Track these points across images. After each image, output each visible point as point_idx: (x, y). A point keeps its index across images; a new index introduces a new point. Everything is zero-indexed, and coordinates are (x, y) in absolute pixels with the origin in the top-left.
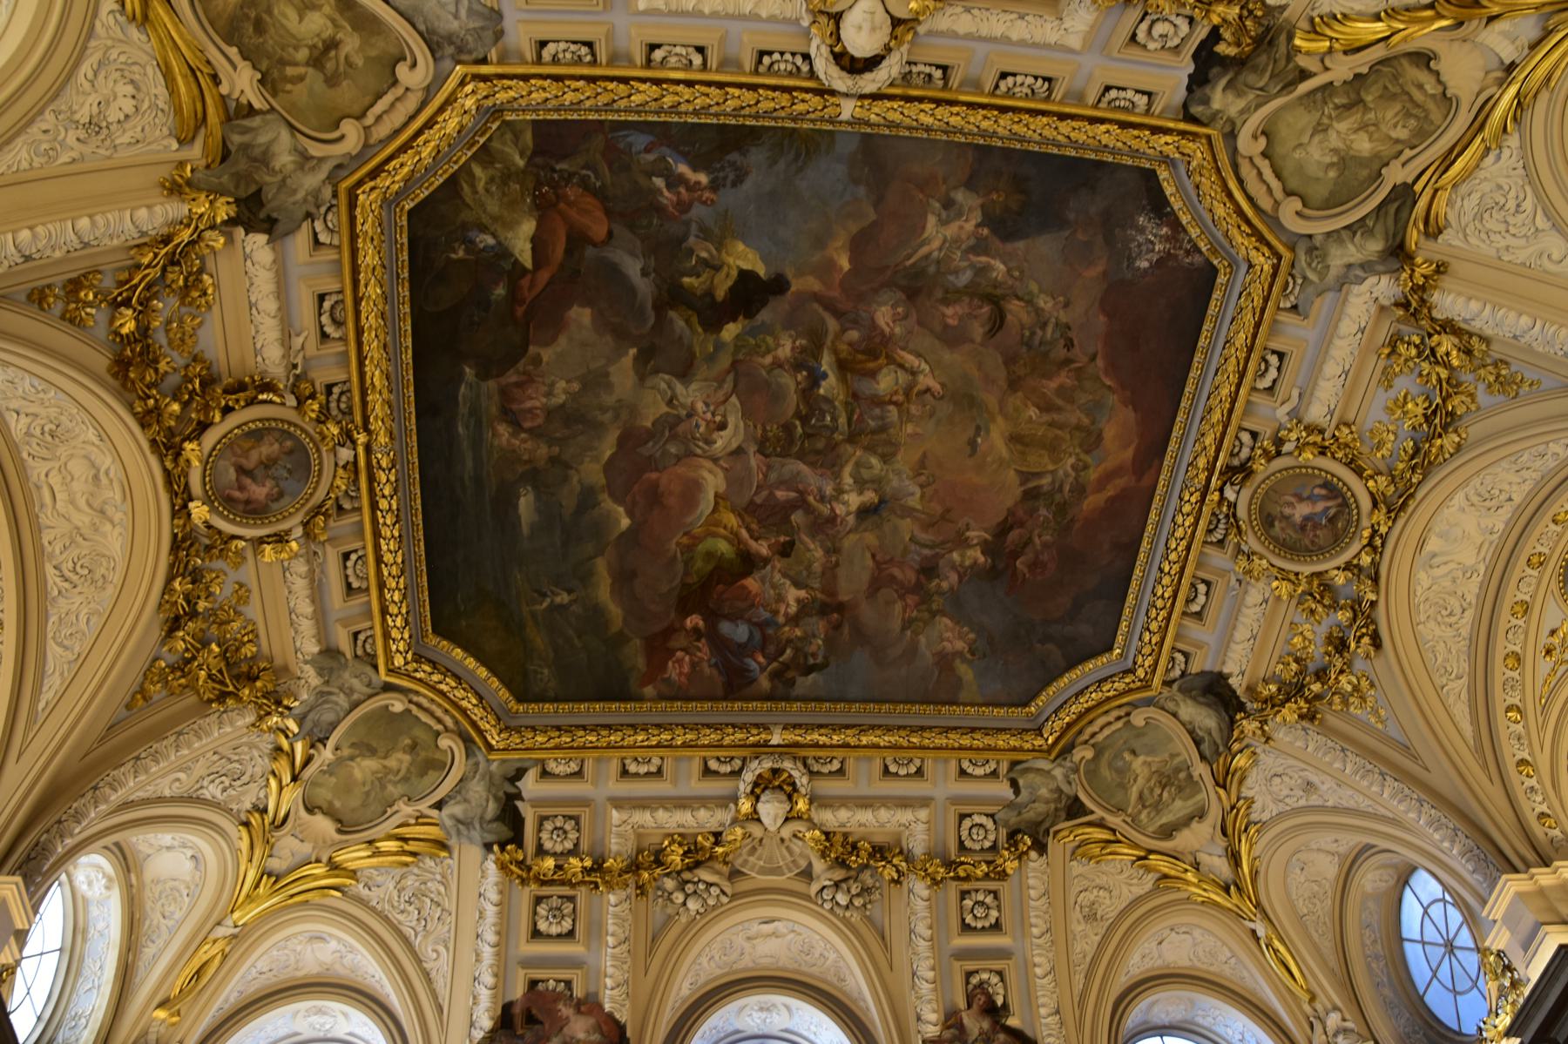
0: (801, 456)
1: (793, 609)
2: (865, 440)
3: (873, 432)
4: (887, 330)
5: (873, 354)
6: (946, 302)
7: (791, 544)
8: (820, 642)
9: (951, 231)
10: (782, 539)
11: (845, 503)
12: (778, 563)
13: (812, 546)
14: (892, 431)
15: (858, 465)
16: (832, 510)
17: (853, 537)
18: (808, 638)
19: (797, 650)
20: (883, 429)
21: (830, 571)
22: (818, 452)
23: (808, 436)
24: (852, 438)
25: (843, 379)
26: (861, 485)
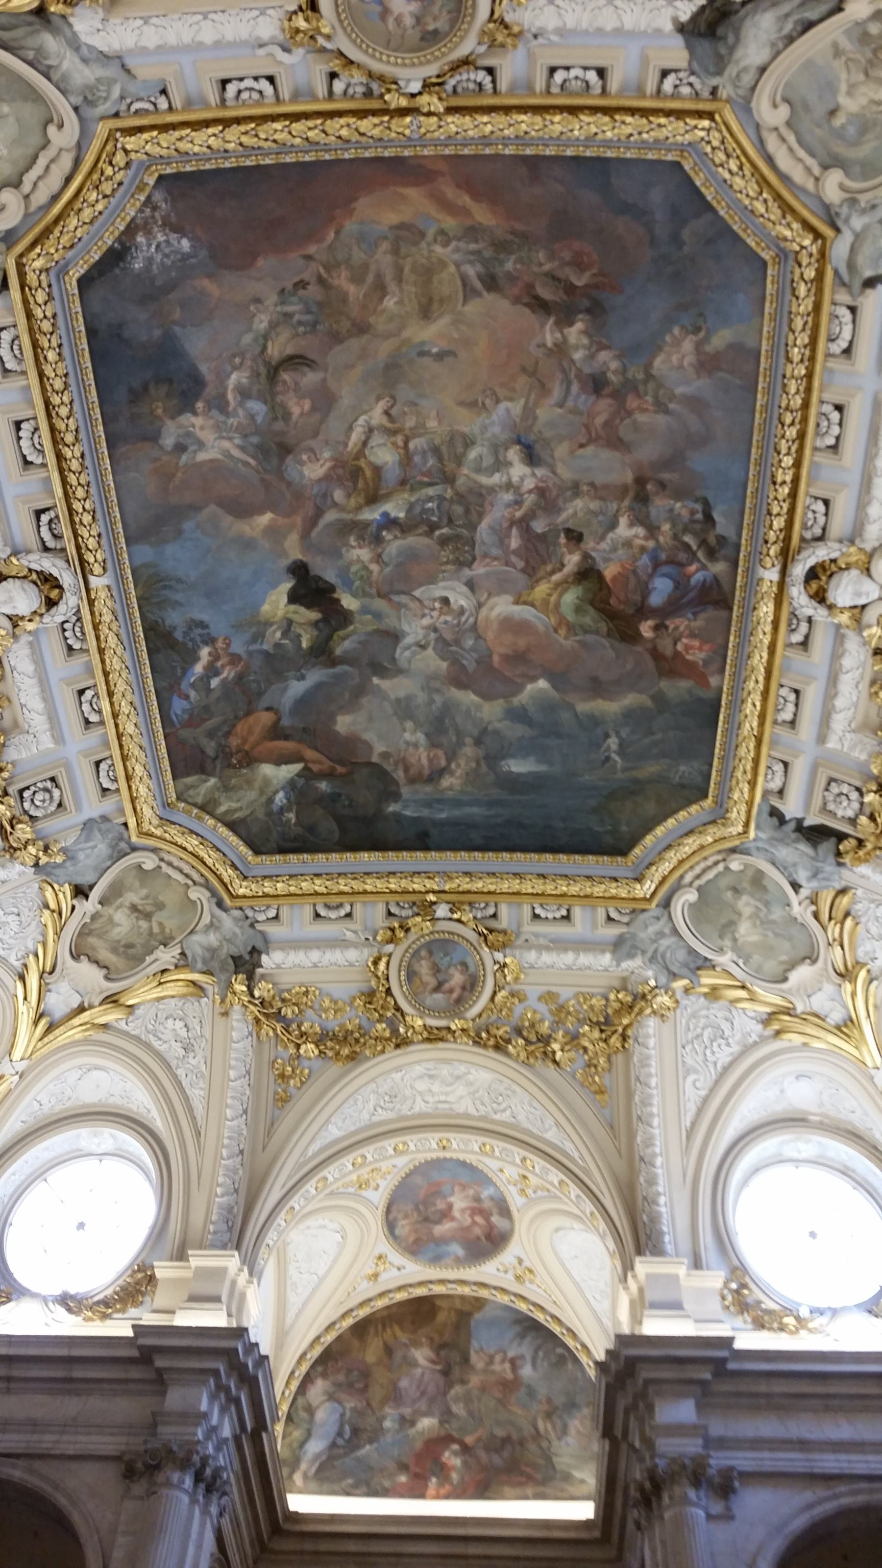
0: (473, 527)
1: (640, 531)
2: (450, 466)
3: (440, 459)
4: (328, 464)
5: (356, 473)
6: (287, 416)
7: (569, 532)
8: (678, 505)
9: (208, 436)
10: (562, 540)
11: (522, 479)
12: (589, 544)
13: (571, 511)
14: (437, 441)
15: (479, 470)
16: (530, 491)
17: (560, 469)
18: (673, 518)
19: (686, 530)
20: (436, 451)
21: (598, 491)
22: (467, 511)
23: (450, 521)
24: (449, 480)
25: (387, 497)
26: (500, 464)
